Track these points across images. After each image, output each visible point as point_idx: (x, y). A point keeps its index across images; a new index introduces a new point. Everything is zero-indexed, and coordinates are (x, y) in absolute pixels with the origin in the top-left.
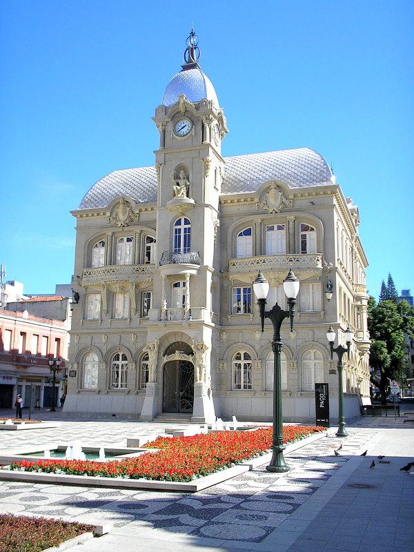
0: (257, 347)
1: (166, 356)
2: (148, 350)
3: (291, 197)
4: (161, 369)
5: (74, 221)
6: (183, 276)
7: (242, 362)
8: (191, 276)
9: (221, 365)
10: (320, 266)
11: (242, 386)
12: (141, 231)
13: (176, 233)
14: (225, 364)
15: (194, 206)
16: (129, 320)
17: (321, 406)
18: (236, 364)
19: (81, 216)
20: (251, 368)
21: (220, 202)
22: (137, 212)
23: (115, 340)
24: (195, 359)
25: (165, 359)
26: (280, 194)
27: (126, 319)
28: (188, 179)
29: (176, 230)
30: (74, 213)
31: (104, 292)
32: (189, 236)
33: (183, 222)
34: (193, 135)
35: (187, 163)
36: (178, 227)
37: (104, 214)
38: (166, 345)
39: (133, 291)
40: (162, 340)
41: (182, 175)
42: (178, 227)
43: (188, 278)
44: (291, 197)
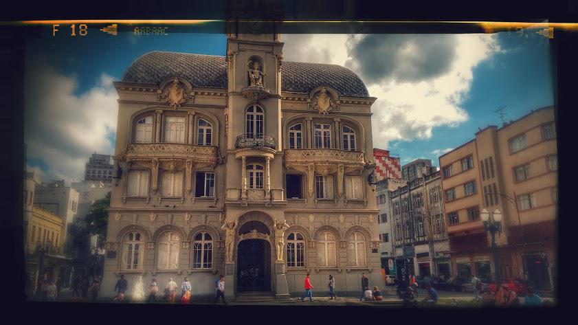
1: (242, 235)
3: (338, 102)
6: (263, 160)
10: (363, 162)
11: (296, 264)
12: (196, 113)
13: (248, 118)
18: (289, 244)
22: (192, 94)
24: (273, 238)
25: (242, 238)
29: (248, 116)
31: (155, 170)
35: (261, 55)
39: (189, 171)
40: (241, 218)
42: (250, 113)
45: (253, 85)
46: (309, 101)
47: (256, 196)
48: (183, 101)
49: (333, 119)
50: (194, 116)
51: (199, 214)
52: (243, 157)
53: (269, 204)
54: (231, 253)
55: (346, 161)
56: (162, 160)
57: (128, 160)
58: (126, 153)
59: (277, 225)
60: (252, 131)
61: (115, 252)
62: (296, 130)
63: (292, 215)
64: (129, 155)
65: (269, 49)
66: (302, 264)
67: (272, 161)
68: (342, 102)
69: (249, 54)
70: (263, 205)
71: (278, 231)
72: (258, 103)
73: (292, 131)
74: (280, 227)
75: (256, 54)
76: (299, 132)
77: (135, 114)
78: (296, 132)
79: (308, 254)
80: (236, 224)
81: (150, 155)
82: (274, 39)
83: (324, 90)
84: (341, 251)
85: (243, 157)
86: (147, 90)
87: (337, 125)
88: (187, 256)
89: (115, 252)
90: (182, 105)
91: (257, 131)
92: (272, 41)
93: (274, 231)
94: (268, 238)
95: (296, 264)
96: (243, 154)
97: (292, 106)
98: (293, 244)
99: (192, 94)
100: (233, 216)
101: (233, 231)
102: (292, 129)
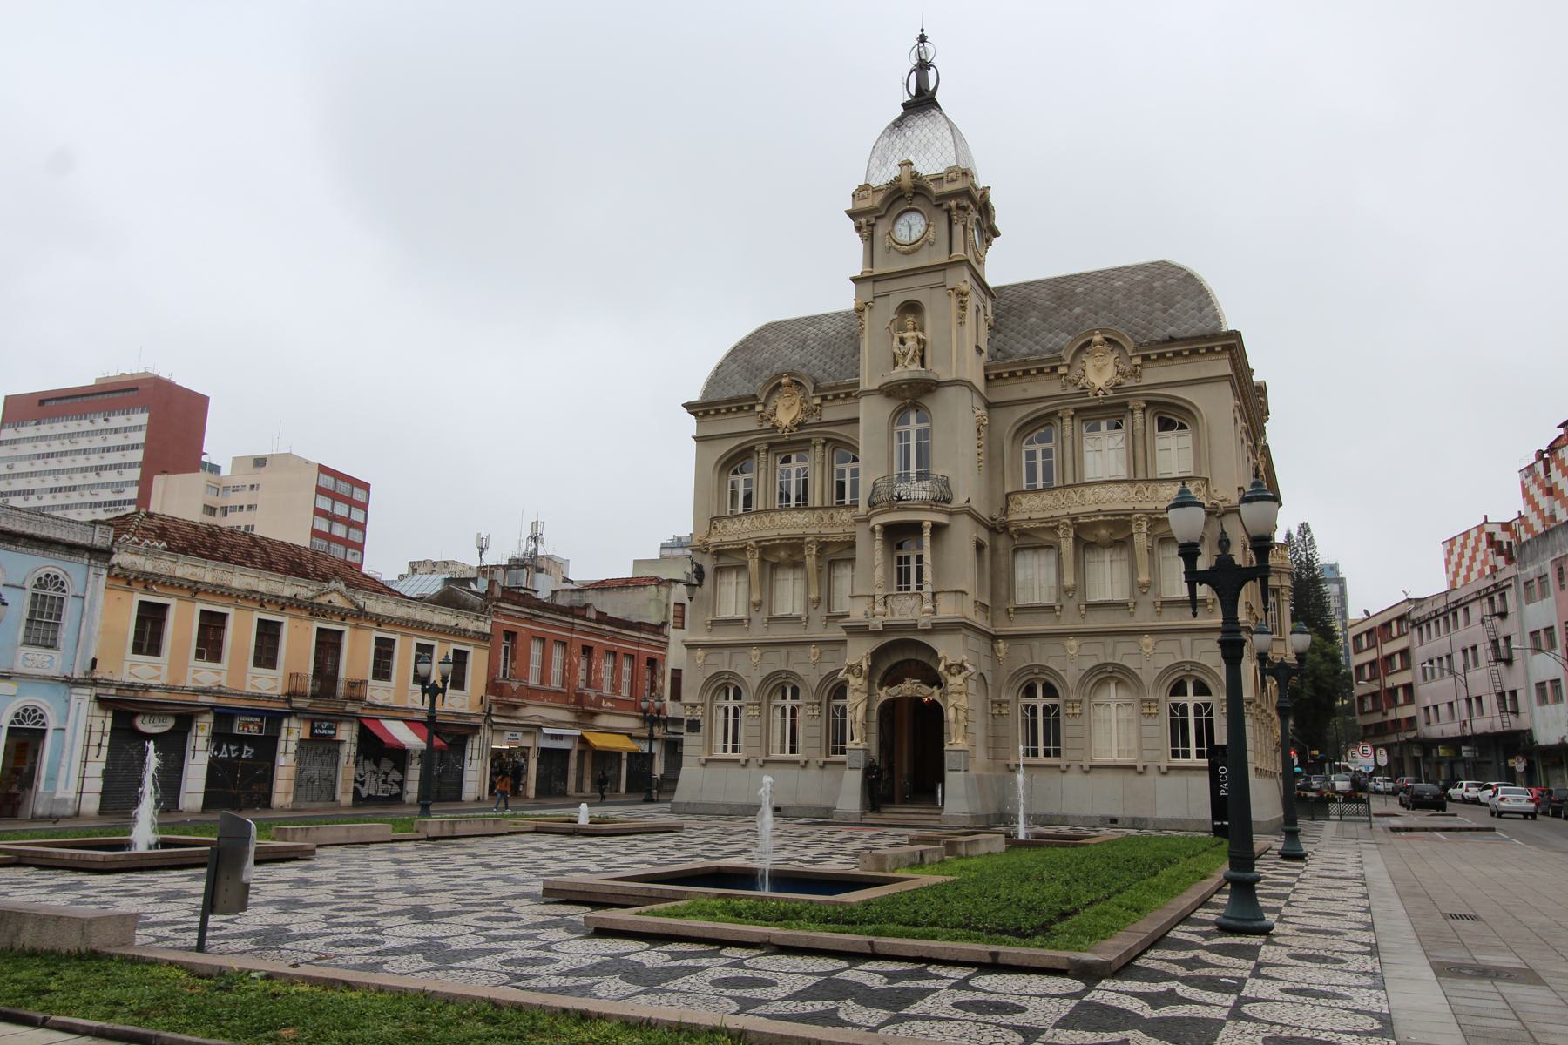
1: (885, 688)
3: (1138, 361)
4: (875, 716)
5: (690, 423)
7: (1040, 701)
11: (1041, 752)
12: (828, 440)
16: (804, 619)
17: (1223, 793)
19: (706, 413)
20: (1057, 714)
23: (777, 661)
24: (945, 695)
25: (884, 694)
27: (799, 618)
29: (900, 433)
30: (689, 407)
31: (753, 564)
32: (927, 445)
37: (752, 407)
40: (877, 656)
42: (903, 428)
43: (927, 532)
45: (898, 369)
46: (1062, 370)
47: (907, 610)
48: (800, 418)
49: (1126, 405)
50: (824, 445)
51: (836, 647)
52: (877, 528)
53: (925, 624)
54: (858, 727)
55: (1151, 506)
56: (763, 543)
57: (712, 550)
58: (709, 535)
59: (948, 668)
60: (907, 467)
61: (699, 721)
62: (1040, 442)
63: (1027, 641)
64: (712, 540)
65: (936, 278)
66: (1057, 753)
67: (937, 529)
68: (1145, 358)
69: (896, 300)
70: (912, 627)
71: (951, 680)
73: (1030, 448)
74: (954, 670)
75: (911, 296)
76: (1047, 446)
77: (721, 458)
78: (1039, 449)
79: (1068, 729)
80: (865, 667)
81: (742, 537)
82: (951, 252)
83: (1098, 338)
84: (1144, 722)
85: (877, 528)
86: (740, 409)
87: (1138, 415)
88: (816, 731)
89: (699, 721)
90: (800, 425)
91: (919, 465)
92: (943, 258)
93: (946, 682)
94: (936, 694)
95: (1041, 752)
96: (877, 522)
97: (1025, 390)
99: (817, 401)
100: (859, 652)
101: (860, 680)
102: (1031, 442)
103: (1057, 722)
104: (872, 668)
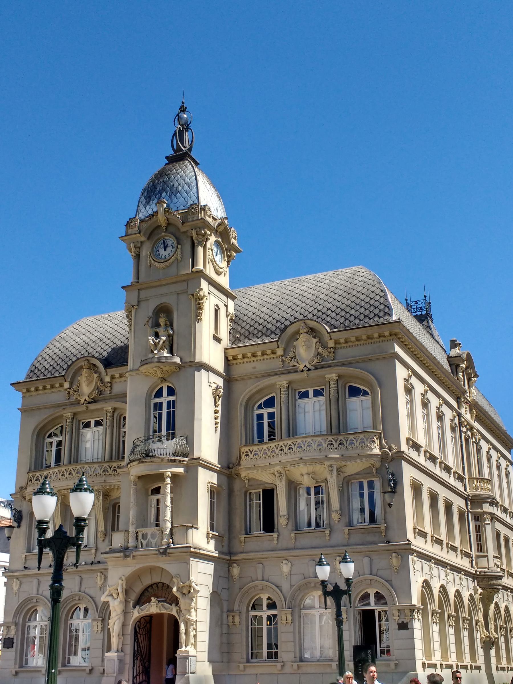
0: (286, 587)
2: (109, 599)
8: (175, 477)
9: (231, 618)
10: (376, 451)
11: (265, 654)
14: (237, 619)
15: (179, 367)
21: (226, 359)
25: (136, 614)
26: (315, 340)
28: (172, 325)
32: (174, 412)
33: (165, 392)
34: (179, 258)
35: (171, 301)
36: (158, 400)
38: (138, 589)
41: (162, 321)
43: (168, 481)
44: (331, 344)
72: (164, 380)
75: (164, 300)
98: (261, 617)
103: (276, 629)
104: (127, 592)
